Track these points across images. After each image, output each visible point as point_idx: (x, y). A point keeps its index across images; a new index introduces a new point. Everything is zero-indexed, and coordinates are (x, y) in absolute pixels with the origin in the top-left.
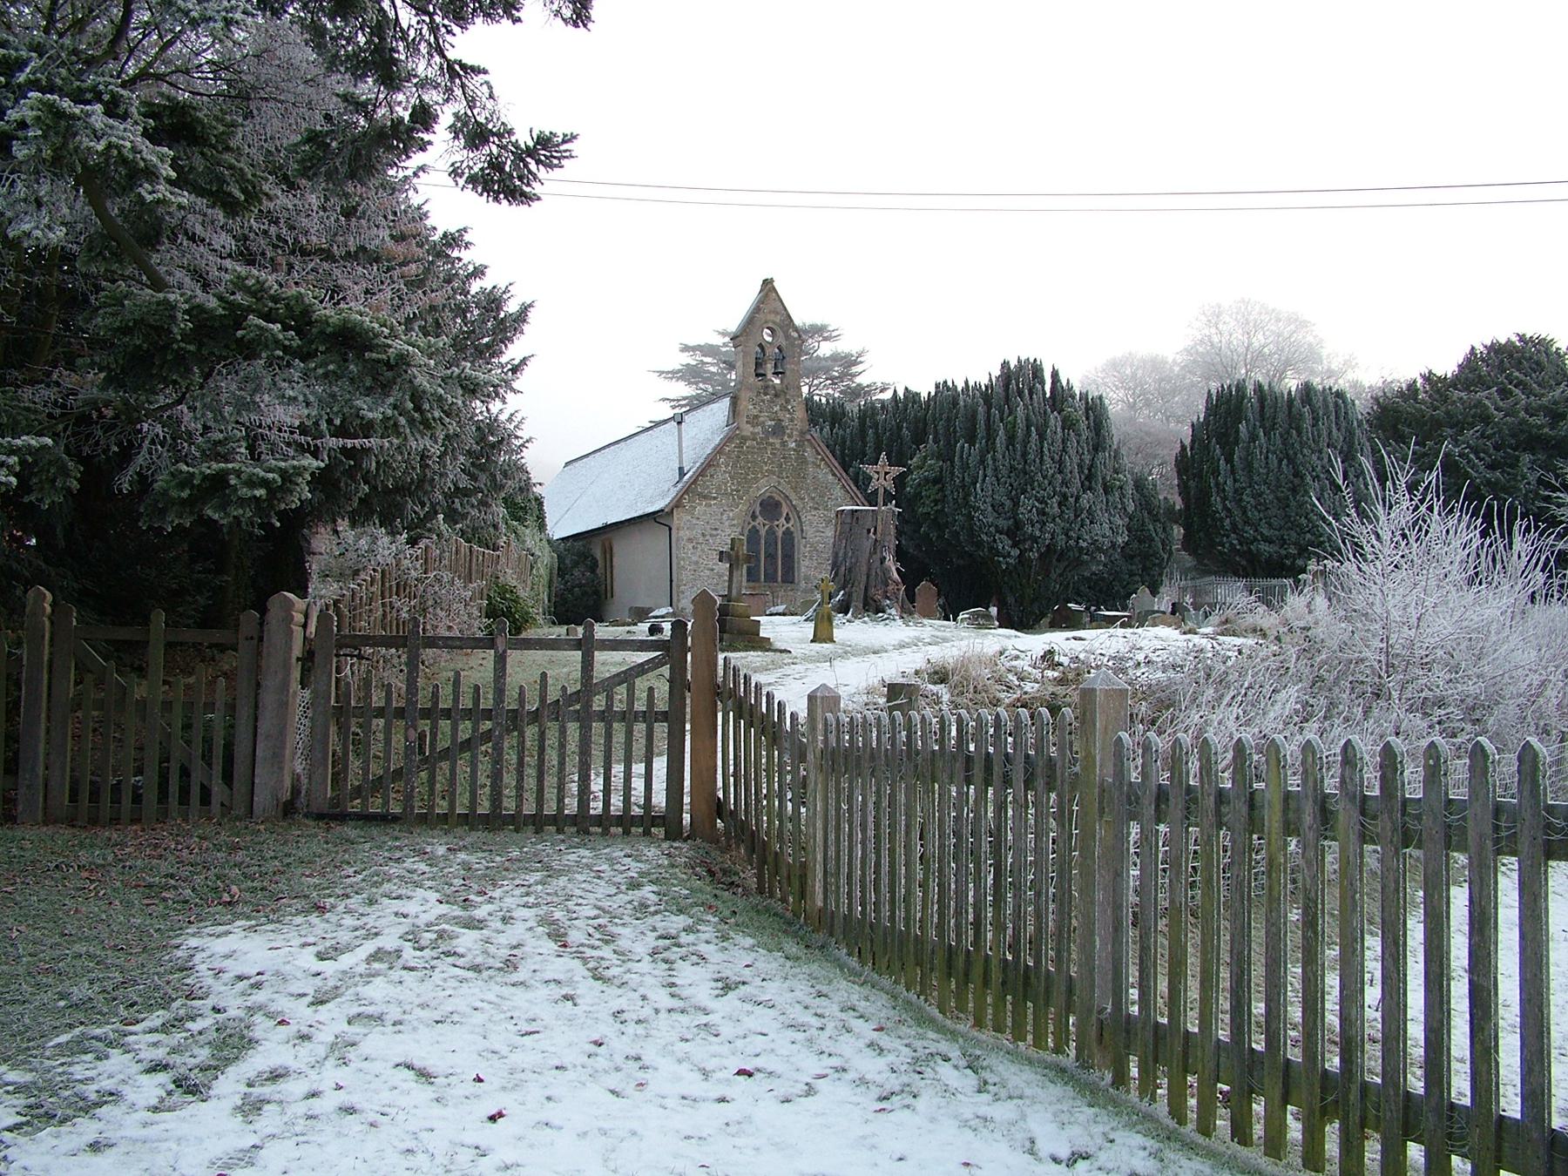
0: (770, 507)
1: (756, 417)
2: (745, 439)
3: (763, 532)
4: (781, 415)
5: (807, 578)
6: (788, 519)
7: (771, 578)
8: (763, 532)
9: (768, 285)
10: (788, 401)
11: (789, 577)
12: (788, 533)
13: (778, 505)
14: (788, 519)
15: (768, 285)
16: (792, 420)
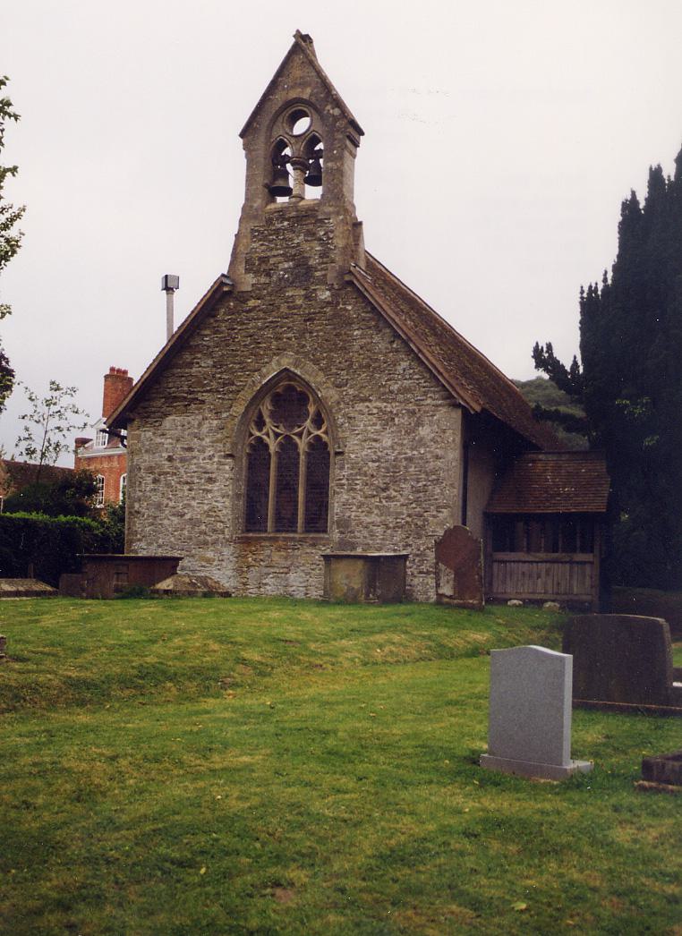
3: (273, 447)
5: (344, 524)
7: (285, 522)
9: (302, 46)
11: (317, 519)
12: (318, 447)
14: (318, 422)
15: (302, 46)
16: (324, 255)
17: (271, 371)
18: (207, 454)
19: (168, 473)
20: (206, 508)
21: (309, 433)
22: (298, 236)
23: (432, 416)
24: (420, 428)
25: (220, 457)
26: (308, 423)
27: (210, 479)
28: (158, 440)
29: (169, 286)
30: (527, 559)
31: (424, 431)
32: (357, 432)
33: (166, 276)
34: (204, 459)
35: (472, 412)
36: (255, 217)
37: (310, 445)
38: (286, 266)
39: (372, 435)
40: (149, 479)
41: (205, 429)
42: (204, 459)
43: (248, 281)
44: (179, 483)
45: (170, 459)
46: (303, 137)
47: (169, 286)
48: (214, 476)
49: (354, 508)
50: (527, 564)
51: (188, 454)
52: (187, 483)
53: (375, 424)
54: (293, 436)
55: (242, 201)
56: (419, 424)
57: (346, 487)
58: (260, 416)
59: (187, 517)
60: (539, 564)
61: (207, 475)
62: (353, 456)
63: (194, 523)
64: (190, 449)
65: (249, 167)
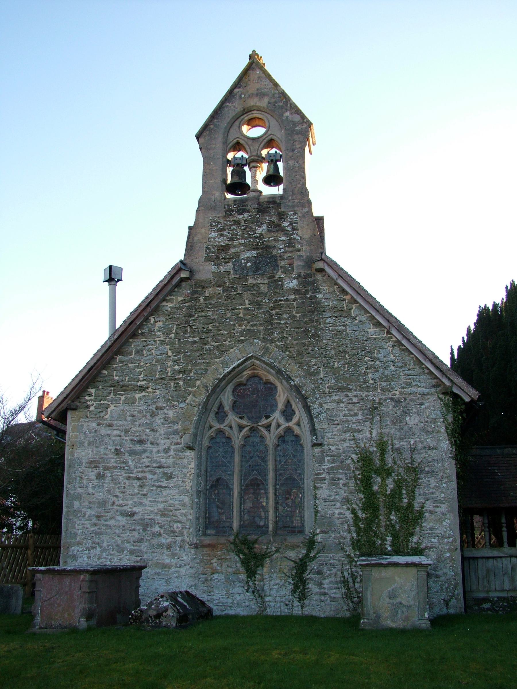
0: (252, 394)
1: (225, 248)
2: (202, 286)
3: (237, 440)
4: (269, 238)
6: (288, 413)
8: (237, 440)
9: (254, 63)
10: (281, 216)
12: (289, 437)
13: (270, 388)
17: (235, 357)
18: (161, 448)
19: (116, 468)
20: (161, 506)
21: (278, 426)
22: (260, 226)
23: (422, 404)
24: (408, 418)
25: (175, 450)
26: (277, 416)
27: (165, 474)
28: (104, 431)
29: (113, 277)
30: (491, 555)
31: (412, 421)
32: (336, 422)
33: (110, 267)
34: (158, 452)
35: (467, 399)
36: (214, 208)
37: (281, 438)
38: (248, 254)
39: (354, 426)
40: (92, 475)
41: (159, 420)
42: (158, 452)
43: (207, 271)
44: (128, 478)
45: (117, 452)
46: (261, 139)
47: (113, 277)
48: (170, 471)
49: (338, 505)
50: (491, 560)
51: (138, 447)
52: (138, 479)
53: (356, 415)
54: (260, 428)
55: (199, 193)
56: (406, 413)
57: (326, 482)
58: (221, 406)
59: (136, 517)
60: (504, 559)
61: (161, 470)
62: (333, 448)
63: (146, 525)
64: (141, 442)
65: (206, 163)
